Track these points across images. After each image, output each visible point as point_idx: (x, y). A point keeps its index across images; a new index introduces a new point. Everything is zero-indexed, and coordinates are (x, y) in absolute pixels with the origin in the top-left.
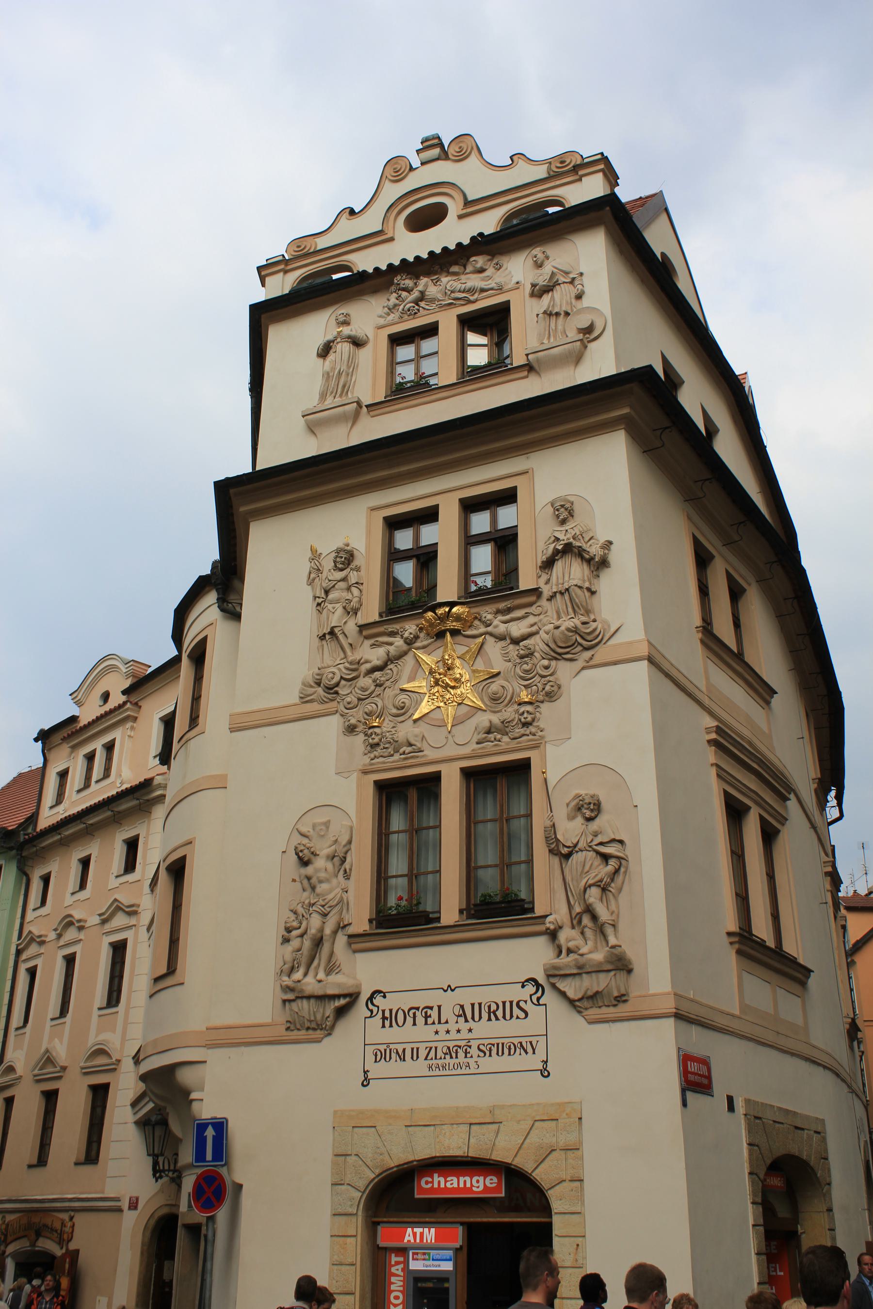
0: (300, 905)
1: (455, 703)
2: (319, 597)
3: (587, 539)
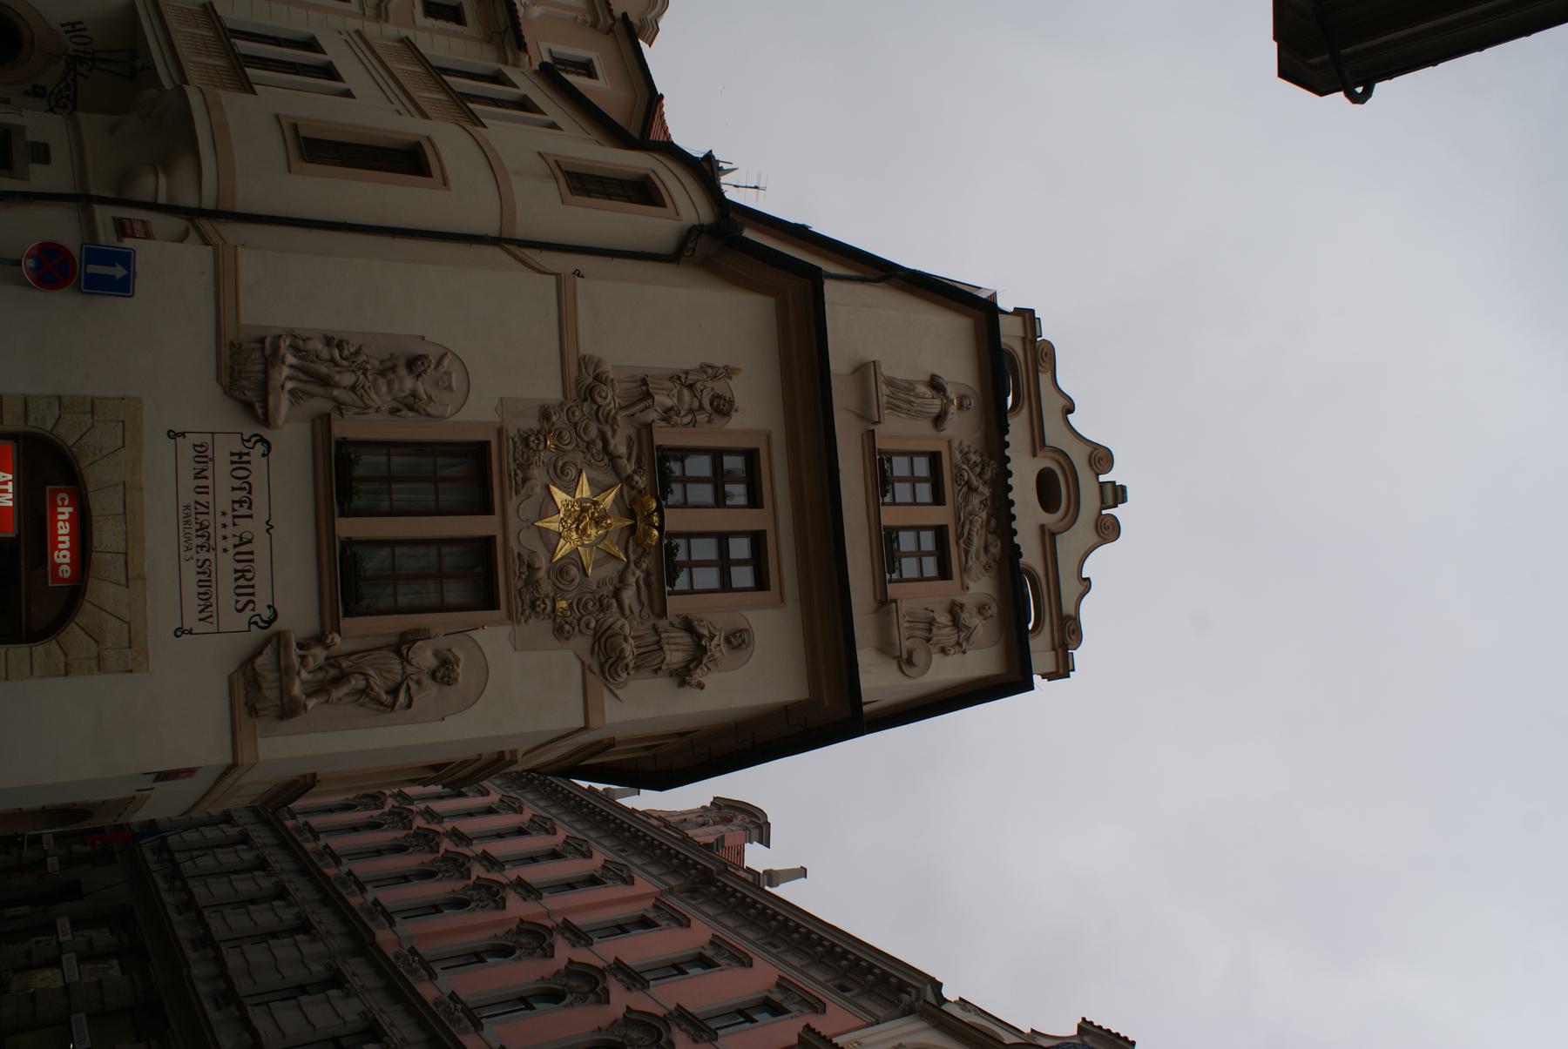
0: (366, 358)
1: (561, 529)
2: (686, 378)
3: (709, 665)
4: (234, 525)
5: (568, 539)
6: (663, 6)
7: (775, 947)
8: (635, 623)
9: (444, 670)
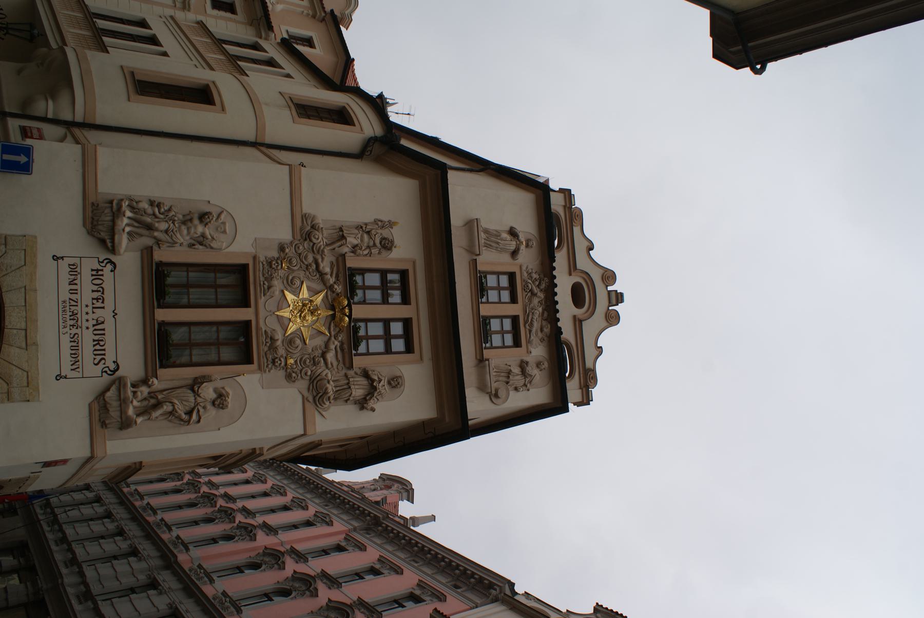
1: (291, 316)
2: (366, 227)
3: (378, 397)
4: (93, 313)
5: (295, 322)
6: (355, 6)
7: (417, 562)
8: (334, 372)
9: (220, 401)
